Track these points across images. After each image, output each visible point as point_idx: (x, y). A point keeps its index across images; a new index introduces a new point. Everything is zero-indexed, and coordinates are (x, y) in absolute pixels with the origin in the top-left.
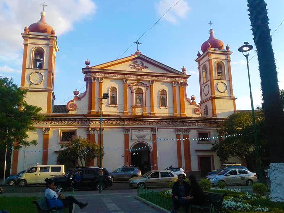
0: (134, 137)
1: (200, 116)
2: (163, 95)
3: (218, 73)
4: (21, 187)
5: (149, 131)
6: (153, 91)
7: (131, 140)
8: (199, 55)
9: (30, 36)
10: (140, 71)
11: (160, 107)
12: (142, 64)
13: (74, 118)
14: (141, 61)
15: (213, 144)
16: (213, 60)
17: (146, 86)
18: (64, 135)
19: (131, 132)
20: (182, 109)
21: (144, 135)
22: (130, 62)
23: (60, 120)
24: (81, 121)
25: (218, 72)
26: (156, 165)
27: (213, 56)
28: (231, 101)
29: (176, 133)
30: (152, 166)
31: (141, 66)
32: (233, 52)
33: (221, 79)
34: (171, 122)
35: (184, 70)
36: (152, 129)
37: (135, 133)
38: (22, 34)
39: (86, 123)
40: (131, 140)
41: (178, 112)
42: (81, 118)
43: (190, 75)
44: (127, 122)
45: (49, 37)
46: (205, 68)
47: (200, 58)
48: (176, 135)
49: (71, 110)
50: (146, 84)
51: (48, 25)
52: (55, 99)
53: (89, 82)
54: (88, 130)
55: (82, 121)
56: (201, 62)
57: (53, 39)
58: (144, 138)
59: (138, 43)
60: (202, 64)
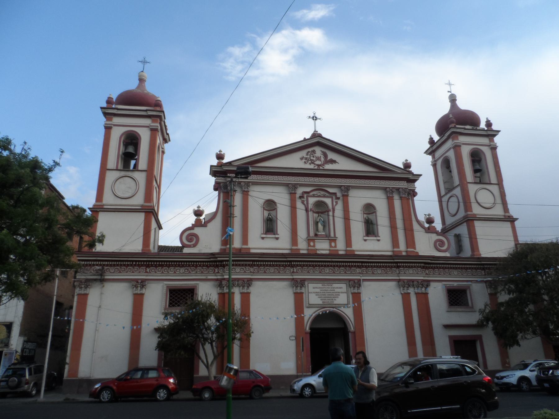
0: (314, 299)
1: (447, 254)
2: (368, 215)
3: (476, 171)
4: (104, 402)
5: (344, 286)
7: (307, 305)
8: (431, 141)
9: (115, 111)
10: (321, 168)
12: (325, 155)
13: (194, 262)
15: (481, 312)
16: (461, 146)
18: (174, 295)
20: (410, 241)
21: (334, 294)
22: (303, 153)
23: (166, 266)
24: (207, 266)
27: (462, 139)
28: (508, 224)
29: (402, 288)
31: (323, 159)
32: (499, 131)
33: (480, 183)
34: (389, 267)
35: (407, 166)
36: (351, 283)
37: (318, 290)
38: (102, 108)
39: (216, 271)
40: (307, 305)
41: (402, 247)
43: (421, 175)
44: (299, 268)
45: (150, 113)
46: (447, 163)
47: (435, 147)
49: (189, 246)
50: (335, 194)
51: (151, 93)
52: (160, 227)
54: (220, 286)
56: (438, 154)
57: (160, 117)
58: (333, 302)
59: (315, 118)
60: (440, 158)
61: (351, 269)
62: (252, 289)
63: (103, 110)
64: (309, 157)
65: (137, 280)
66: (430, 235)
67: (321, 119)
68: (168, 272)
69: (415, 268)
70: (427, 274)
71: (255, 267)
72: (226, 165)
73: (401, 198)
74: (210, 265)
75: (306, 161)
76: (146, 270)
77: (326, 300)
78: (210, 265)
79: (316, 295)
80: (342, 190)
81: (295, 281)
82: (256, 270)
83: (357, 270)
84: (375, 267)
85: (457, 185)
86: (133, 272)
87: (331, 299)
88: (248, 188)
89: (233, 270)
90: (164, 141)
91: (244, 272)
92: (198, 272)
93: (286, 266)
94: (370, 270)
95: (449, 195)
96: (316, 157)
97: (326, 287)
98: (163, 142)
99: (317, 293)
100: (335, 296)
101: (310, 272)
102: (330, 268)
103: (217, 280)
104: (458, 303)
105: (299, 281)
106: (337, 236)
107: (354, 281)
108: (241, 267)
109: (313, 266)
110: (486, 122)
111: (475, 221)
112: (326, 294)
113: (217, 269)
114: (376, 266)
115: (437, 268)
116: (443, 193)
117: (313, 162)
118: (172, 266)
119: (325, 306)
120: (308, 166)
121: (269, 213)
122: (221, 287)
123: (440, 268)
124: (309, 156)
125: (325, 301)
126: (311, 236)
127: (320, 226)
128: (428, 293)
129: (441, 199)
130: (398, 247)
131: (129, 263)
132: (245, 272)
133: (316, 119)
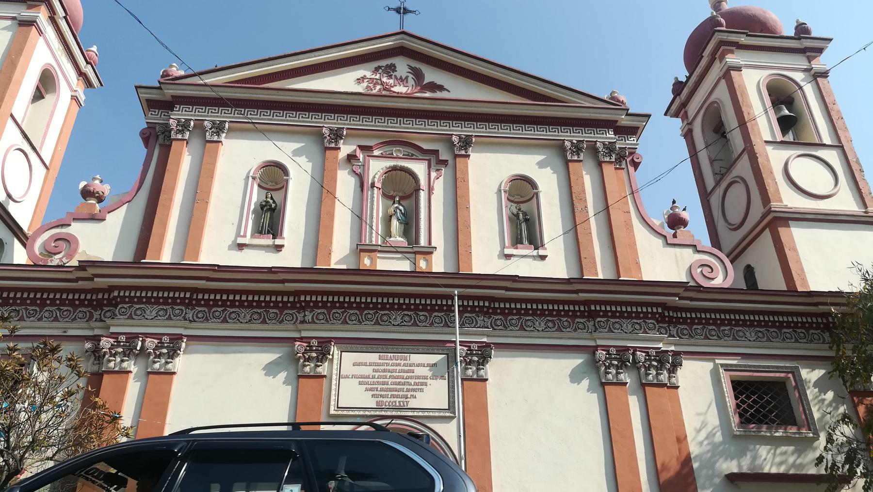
6: (466, 181)
7: (336, 413)
11: (507, 251)
12: (418, 75)
19: (335, 367)
21: (412, 381)
24: (72, 303)
25: (778, 116)
31: (411, 82)
32: (830, 40)
37: (368, 371)
42: (68, 291)
43: (649, 116)
44: (319, 311)
50: (436, 152)
53: (160, 144)
55: (75, 307)
59: (402, 11)
62: (180, 363)
64: (378, 77)
66: (678, 250)
67: (417, 13)
69: (640, 318)
70: (671, 336)
71: (200, 309)
72: (173, 82)
73: (600, 164)
74: (79, 299)
75: (369, 85)
77: (386, 396)
78: (79, 299)
81: (305, 344)
82: (200, 315)
83: (477, 318)
84: (527, 312)
85: (740, 151)
87: (401, 393)
88: (218, 135)
89: (139, 312)
90: (81, 78)
91: (167, 319)
93: (286, 305)
94: (513, 322)
95: (724, 185)
97: (391, 362)
99: (362, 377)
100: (415, 387)
102: (406, 313)
104: (765, 416)
106: (433, 245)
107: (470, 346)
108: (161, 307)
110: (796, 28)
111: (790, 222)
112: (390, 380)
113: (98, 312)
115: (697, 324)
116: (710, 182)
117: (387, 87)
119: (383, 413)
121: (267, 193)
122: (99, 356)
123: (708, 322)
125: (385, 400)
127: (395, 223)
128: (678, 387)
129: (708, 201)
130: (597, 274)
132: (169, 318)
133: (406, 11)
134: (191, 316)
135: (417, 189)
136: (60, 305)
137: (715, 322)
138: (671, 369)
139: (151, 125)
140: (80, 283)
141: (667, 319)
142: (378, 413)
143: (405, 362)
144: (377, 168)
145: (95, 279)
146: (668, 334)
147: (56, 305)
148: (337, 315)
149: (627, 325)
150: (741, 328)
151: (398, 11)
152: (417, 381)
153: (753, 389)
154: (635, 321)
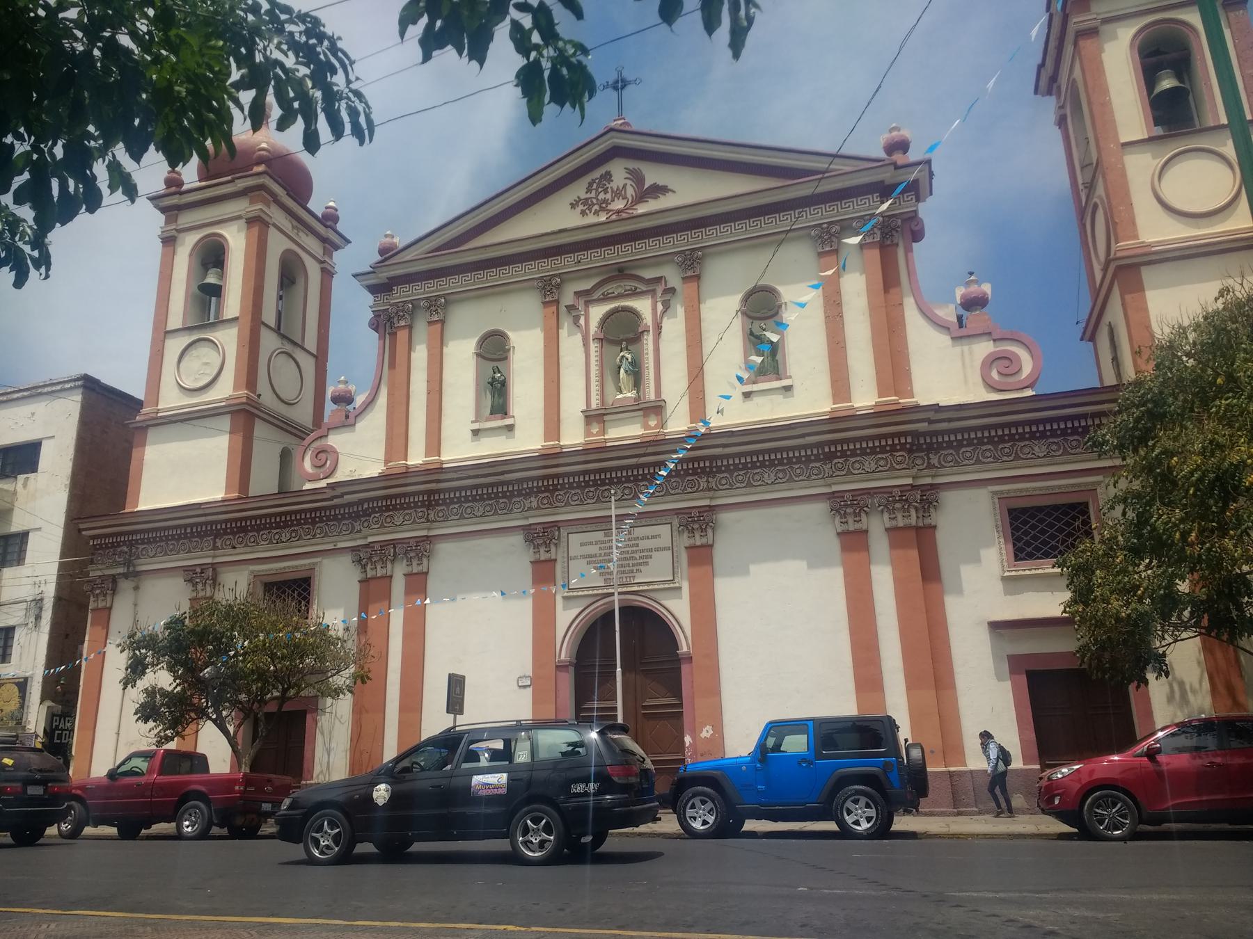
5: (664, 530)
7: (566, 594)
10: (624, 215)
12: (638, 178)
14: (633, 164)
17: (659, 293)
22: (578, 190)
26: (708, 728)
29: (838, 519)
30: (688, 740)
31: (630, 192)
37: (593, 550)
39: (357, 528)
48: (838, 534)
55: (339, 521)
57: (262, 187)
58: (634, 577)
61: (683, 482)
63: (154, 201)
65: (194, 568)
68: (258, 543)
69: (887, 452)
70: (930, 466)
76: (215, 543)
79: (589, 563)
80: (680, 265)
81: (533, 532)
82: (440, 514)
84: (754, 466)
86: (189, 551)
87: (627, 569)
89: (388, 520)
90: (327, 245)
92: (318, 536)
94: (740, 478)
96: (612, 191)
98: (324, 248)
99: (590, 556)
100: (641, 561)
101: (572, 503)
102: (626, 485)
103: (353, 549)
104: (1054, 548)
105: (540, 529)
106: (663, 397)
109: (579, 487)
113: (358, 524)
114: (749, 465)
115: (966, 446)
117: (604, 205)
118: (265, 528)
120: (591, 219)
124: (594, 192)
126: (594, 406)
128: (935, 527)
131: (179, 532)
132: (414, 522)
134: (432, 516)
135: (643, 332)
136: (328, 520)
137: (990, 440)
138: (926, 507)
139: (377, 313)
140: (335, 500)
141: (924, 446)
142: (605, 591)
143: (630, 536)
144: (597, 312)
145: (345, 497)
146: (925, 465)
147: (325, 521)
148: (559, 497)
149: (870, 463)
150: (1027, 443)
151: (616, 88)
152: (642, 554)
153: (1041, 516)
154: (880, 456)
